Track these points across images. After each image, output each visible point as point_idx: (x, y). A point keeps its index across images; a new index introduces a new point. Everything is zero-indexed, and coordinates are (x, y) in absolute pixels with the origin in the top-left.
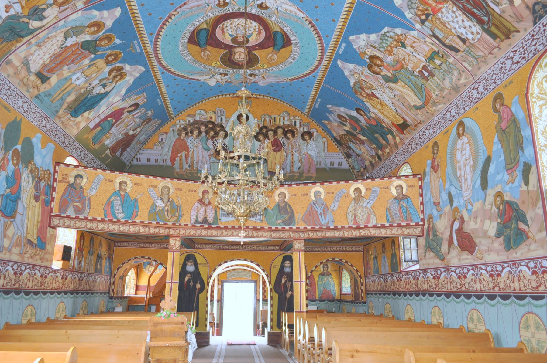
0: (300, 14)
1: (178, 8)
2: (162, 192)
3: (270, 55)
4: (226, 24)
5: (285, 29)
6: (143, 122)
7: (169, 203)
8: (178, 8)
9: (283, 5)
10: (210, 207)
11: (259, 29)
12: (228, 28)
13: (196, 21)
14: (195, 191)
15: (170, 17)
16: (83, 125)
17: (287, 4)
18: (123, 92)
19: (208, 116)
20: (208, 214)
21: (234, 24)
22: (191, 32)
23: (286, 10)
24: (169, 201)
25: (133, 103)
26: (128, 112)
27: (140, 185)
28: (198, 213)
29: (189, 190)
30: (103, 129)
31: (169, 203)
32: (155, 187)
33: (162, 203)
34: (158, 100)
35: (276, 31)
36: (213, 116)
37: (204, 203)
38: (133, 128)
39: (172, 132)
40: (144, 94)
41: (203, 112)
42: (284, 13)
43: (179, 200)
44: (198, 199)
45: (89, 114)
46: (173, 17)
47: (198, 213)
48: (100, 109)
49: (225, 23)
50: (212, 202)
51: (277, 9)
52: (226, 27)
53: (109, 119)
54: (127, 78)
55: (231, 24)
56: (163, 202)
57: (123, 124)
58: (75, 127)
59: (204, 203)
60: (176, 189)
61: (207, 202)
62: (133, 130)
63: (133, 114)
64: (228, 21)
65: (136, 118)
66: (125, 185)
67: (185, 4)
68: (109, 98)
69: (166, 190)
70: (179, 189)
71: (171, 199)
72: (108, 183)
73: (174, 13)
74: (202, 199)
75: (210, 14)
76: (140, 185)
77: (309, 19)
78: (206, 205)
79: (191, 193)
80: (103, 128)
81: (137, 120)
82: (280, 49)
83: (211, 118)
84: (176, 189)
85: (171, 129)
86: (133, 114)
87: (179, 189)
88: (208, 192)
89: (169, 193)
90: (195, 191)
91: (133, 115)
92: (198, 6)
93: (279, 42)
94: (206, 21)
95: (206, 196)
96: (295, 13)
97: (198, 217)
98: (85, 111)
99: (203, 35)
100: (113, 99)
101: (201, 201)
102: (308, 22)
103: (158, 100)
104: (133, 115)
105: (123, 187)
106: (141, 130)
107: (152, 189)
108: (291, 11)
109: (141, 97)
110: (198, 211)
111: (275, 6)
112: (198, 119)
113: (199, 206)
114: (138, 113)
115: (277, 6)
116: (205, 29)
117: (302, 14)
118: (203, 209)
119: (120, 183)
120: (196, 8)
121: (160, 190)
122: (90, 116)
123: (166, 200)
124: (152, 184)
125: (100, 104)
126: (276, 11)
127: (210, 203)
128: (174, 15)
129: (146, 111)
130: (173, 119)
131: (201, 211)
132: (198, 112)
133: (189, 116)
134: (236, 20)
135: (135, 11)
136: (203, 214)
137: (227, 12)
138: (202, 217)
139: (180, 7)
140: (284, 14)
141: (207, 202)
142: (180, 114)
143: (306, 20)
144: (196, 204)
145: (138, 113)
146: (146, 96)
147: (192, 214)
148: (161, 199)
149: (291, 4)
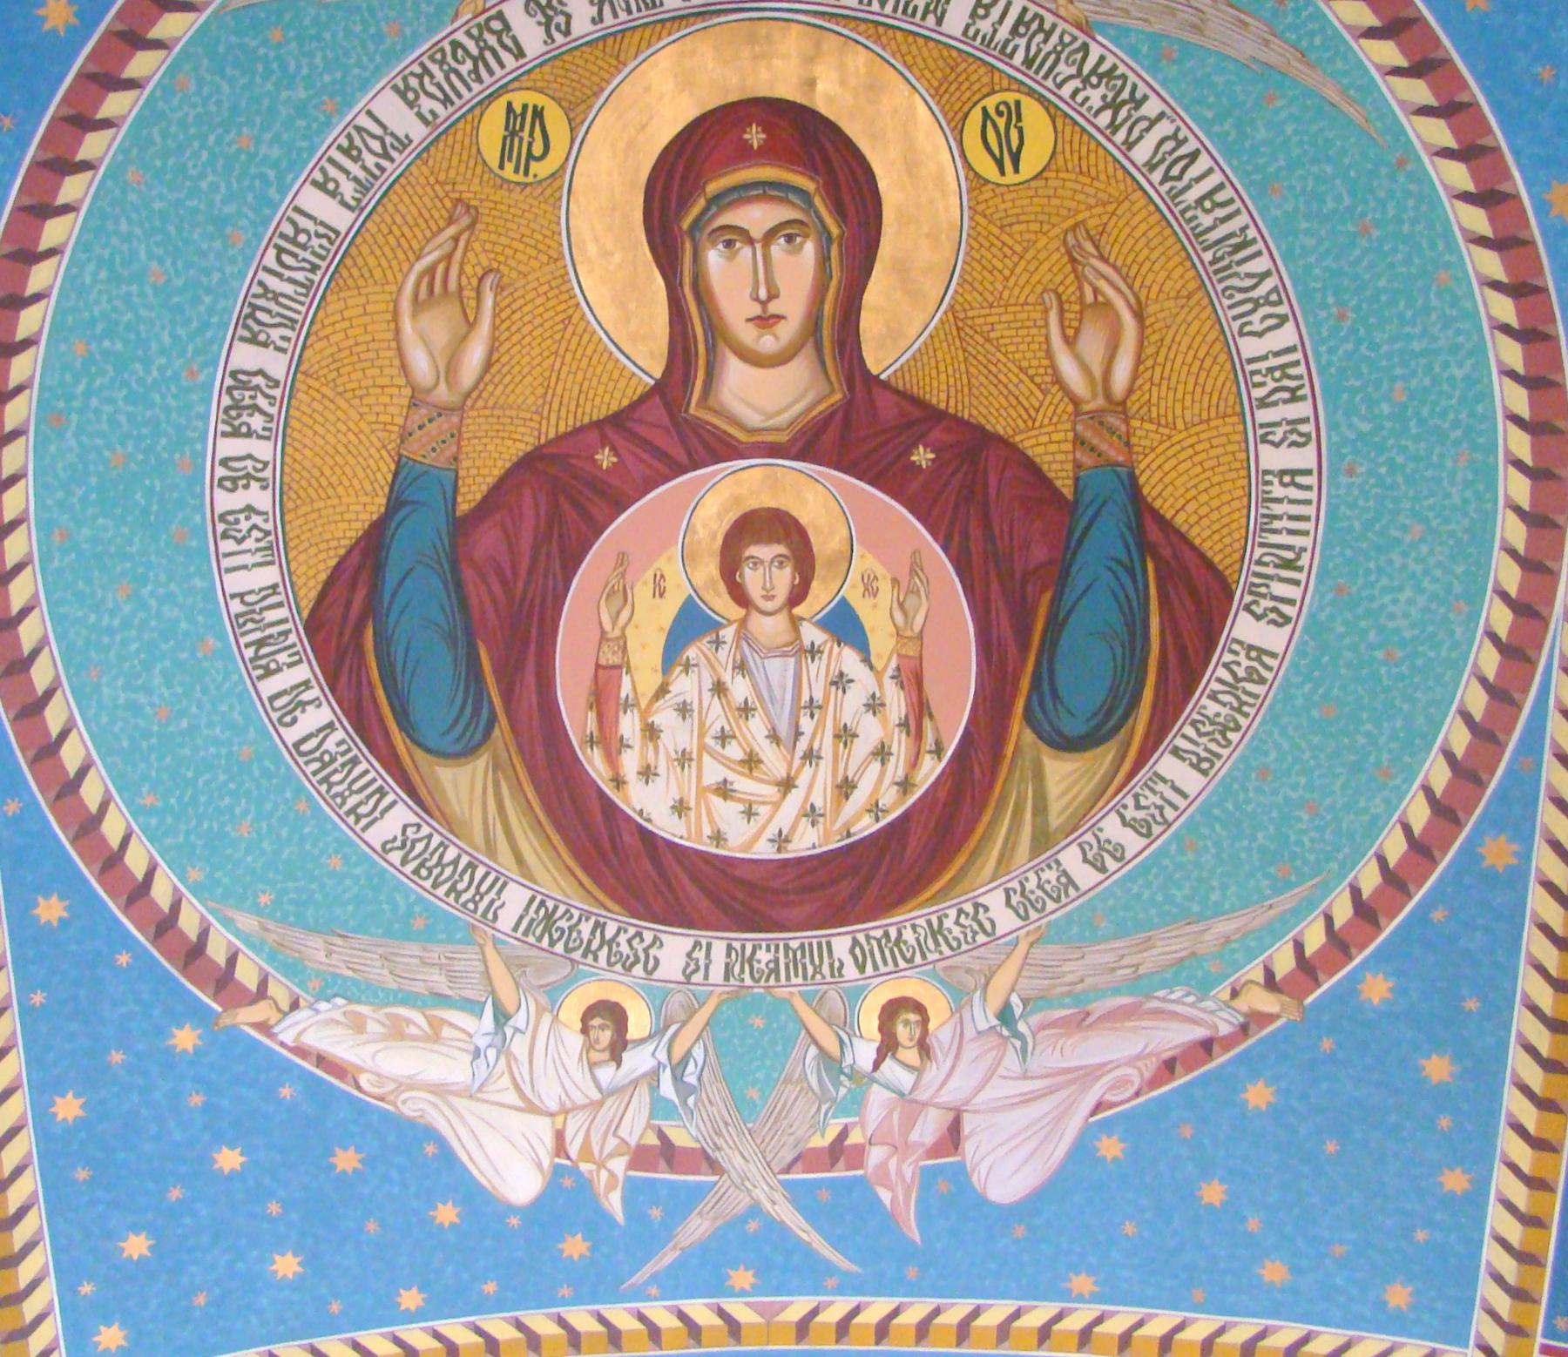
0: (316, 1029)
1: (1229, 1042)
3: (475, 355)
4: (888, 796)
5: (400, 816)
8: (1229, 1042)
9: (452, 1068)
11: (611, 745)
12: (871, 731)
13: (1118, 853)
15: (1308, 969)
17: (440, 1090)
21: (816, 784)
22: (1183, 734)
23: (434, 1035)
35: (466, 752)
42: (441, 999)
46: (1284, 963)
49: (895, 806)
51: (502, 1016)
52: (882, 753)
55: (845, 788)
64: (866, 826)
67: (1169, 1067)
73: (1267, 1003)
75: (1005, 920)
77: (247, 1016)
82: (396, 503)
92: (1080, 1022)
93: (418, 607)
94: (1043, 841)
96: (358, 1025)
99: (1085, 671)
102: (246, 974)
108: (396, 1032)
111: (519, 1046)
115: (503, 1048)
116: (1067, 744)
117: (316, 1039)
120: (1099, 1007)
126: (509, 1005)
128: (1270, 982)
134: (808, 841)
135: (1503, 1304)
137: (875, 928)
139: (1207, 1046)
140: (440, 982)
143: (262, 992)
149: (413, 1106)
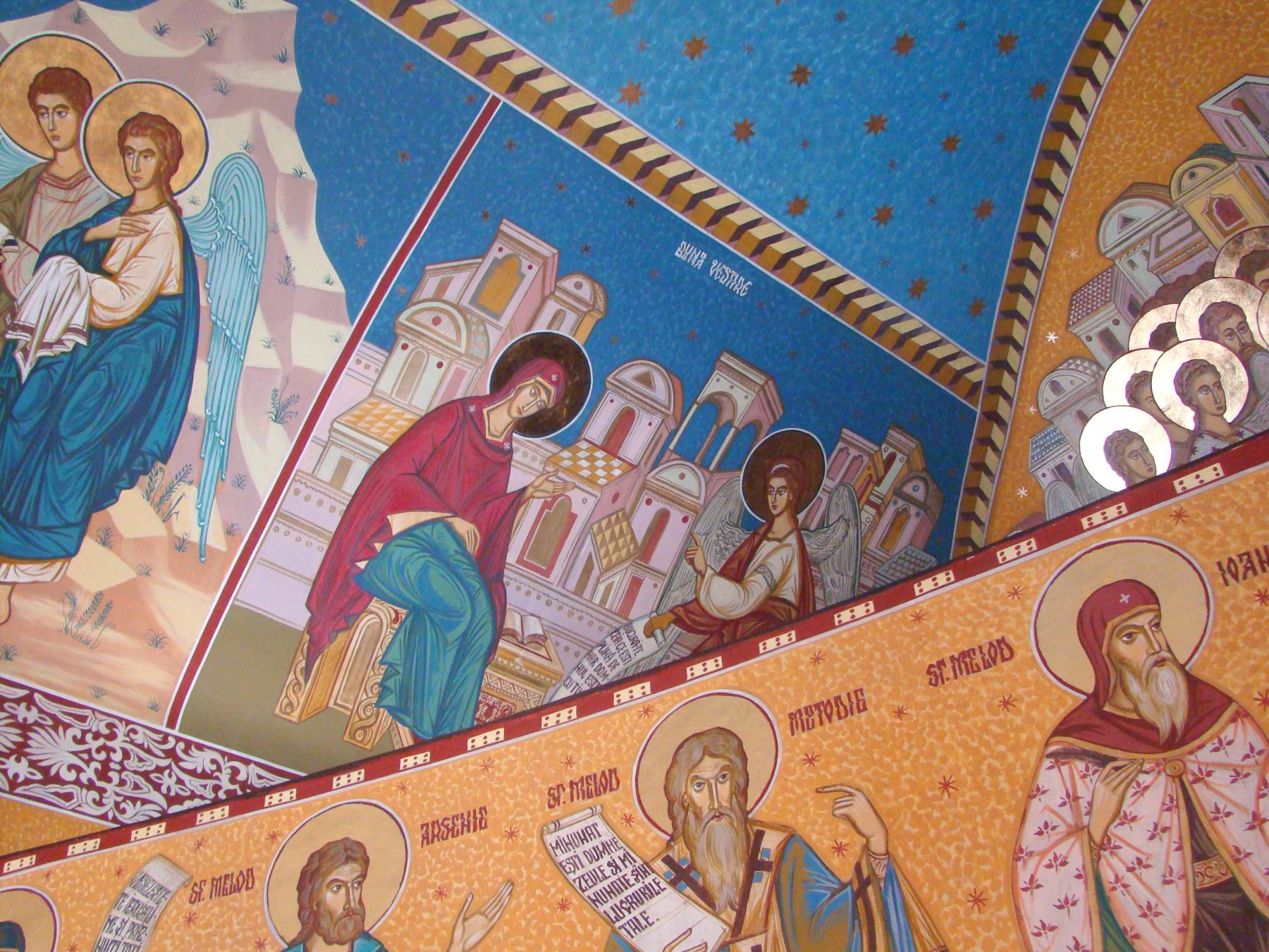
2: (677, 806)
6: (756, 493)
7: (760, 890)
10: (1239, 739)
14: (1000, 650)
16: (184, 612)
18: (312, 265)
19: (1196, 208)
20: (1234, 832)
24: (754, 864)
25: (498, 340)
26: (533, 426)
27: (476, 820)
28: (1111, 867)
29: (935, 674)
30: (419, 617)
31: (760, 890)
32: (606, 782)
33: (695, 914)
34: (684, 252)
36: (1231, 188)
37: (1140, 735)
38: (711, 558)
39: (1063, 488)
40: (507, 227)
41: (1143, 210)
43: (859, 808)
44: (1052, 719)
45: (163, 506)
47: (1111, 867)
48: (228, 450)
50: (1229, 682)
53: (399, 522)
54: (228, 135)
56: (705, 896)
57: (575, 549)
58: (110, 635)
59: (1140, 735)
60: (799, 720)
61: (1163, 699)
62: (736, 571)
63: (598, 428)
65: (658, 456)
66: (347, 872)
68: (236, 350)
69: (709, 768)
70: (830, 709)
71: (771, 841)
72: (210, 908)
74: (1097, 698)
76: (476, 820)
78: (1177, 740)
79: (960, 687)
80: (415, 611)
81: (683, 478)
83: (1227, 210)
84: (799, 720)
85: (1045, 476)
86: (598, 428)
87: (830, 709)
88: (1144, 595)
89: (741, 792)
90: (1000, 650)
91: (612, 444)
95: (1134, 652)
97: (1127, 909)
98: (104, 496)
100: (280, 342)
101: (1099, 727)
103: (684, 252)
104: (612, 444)
105: (334, 900)
106: (806, 562)
107: (577, 818)
109: (507, 270)
110: (1100, 847)
112: (1150, 285)
113: (1095, 788)
114: (625, 421)
118: (1151, 801)
119: (310, 878)
121: (657, 805)
122: (186, 524)
123: (723, 872)
124: (578, 771)
125: (196, 406)
127: (1206, 704)
129: (688, 383)
130: (996, 390)
131: (1134, 836)
132: (1111, 233)
133: (1079, 302)
136: (1167, 854)
138: (1174, 903)
141: (1163, 699)
142: (1018, 332)
144: (1052, 780)
145: (625, 421)
146: (546, 250)
147: (1037, 908)
148: (683, 876)
